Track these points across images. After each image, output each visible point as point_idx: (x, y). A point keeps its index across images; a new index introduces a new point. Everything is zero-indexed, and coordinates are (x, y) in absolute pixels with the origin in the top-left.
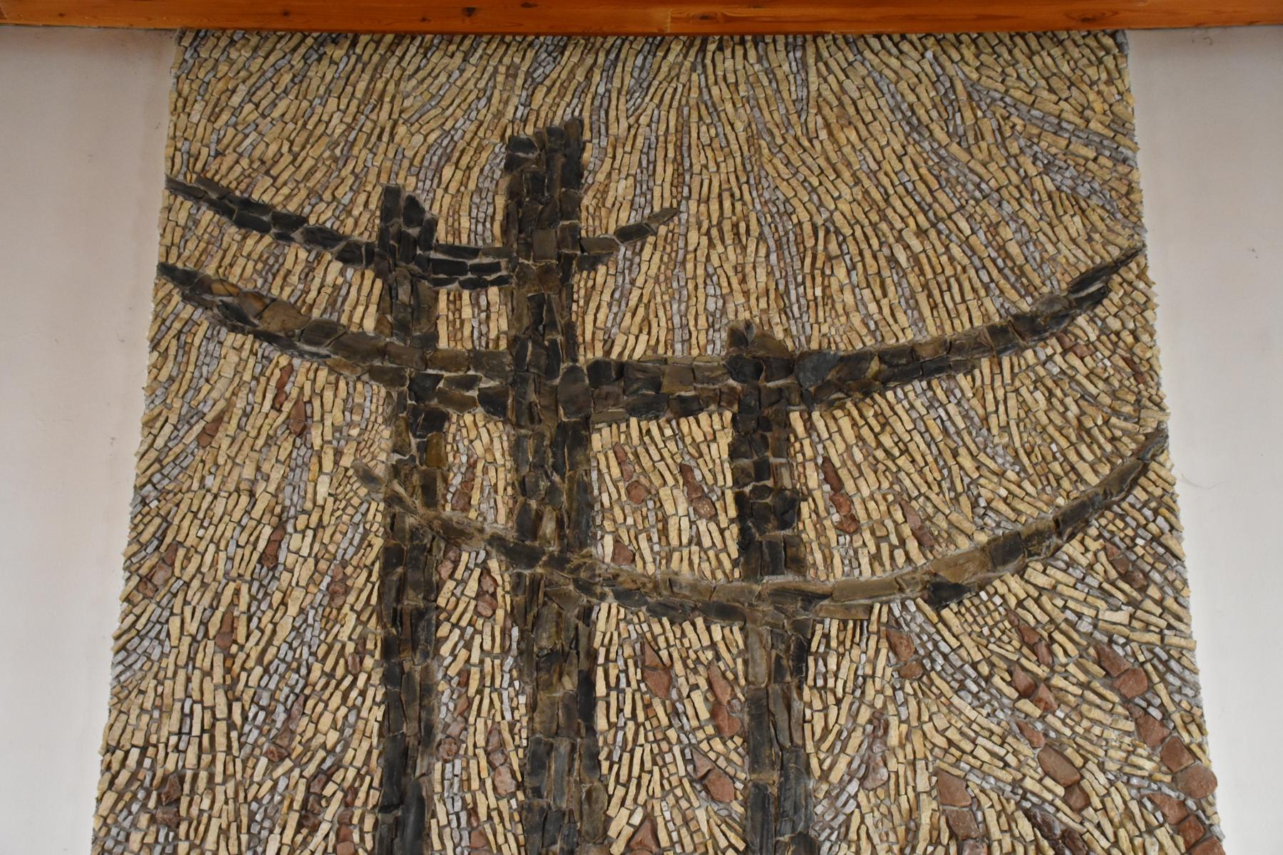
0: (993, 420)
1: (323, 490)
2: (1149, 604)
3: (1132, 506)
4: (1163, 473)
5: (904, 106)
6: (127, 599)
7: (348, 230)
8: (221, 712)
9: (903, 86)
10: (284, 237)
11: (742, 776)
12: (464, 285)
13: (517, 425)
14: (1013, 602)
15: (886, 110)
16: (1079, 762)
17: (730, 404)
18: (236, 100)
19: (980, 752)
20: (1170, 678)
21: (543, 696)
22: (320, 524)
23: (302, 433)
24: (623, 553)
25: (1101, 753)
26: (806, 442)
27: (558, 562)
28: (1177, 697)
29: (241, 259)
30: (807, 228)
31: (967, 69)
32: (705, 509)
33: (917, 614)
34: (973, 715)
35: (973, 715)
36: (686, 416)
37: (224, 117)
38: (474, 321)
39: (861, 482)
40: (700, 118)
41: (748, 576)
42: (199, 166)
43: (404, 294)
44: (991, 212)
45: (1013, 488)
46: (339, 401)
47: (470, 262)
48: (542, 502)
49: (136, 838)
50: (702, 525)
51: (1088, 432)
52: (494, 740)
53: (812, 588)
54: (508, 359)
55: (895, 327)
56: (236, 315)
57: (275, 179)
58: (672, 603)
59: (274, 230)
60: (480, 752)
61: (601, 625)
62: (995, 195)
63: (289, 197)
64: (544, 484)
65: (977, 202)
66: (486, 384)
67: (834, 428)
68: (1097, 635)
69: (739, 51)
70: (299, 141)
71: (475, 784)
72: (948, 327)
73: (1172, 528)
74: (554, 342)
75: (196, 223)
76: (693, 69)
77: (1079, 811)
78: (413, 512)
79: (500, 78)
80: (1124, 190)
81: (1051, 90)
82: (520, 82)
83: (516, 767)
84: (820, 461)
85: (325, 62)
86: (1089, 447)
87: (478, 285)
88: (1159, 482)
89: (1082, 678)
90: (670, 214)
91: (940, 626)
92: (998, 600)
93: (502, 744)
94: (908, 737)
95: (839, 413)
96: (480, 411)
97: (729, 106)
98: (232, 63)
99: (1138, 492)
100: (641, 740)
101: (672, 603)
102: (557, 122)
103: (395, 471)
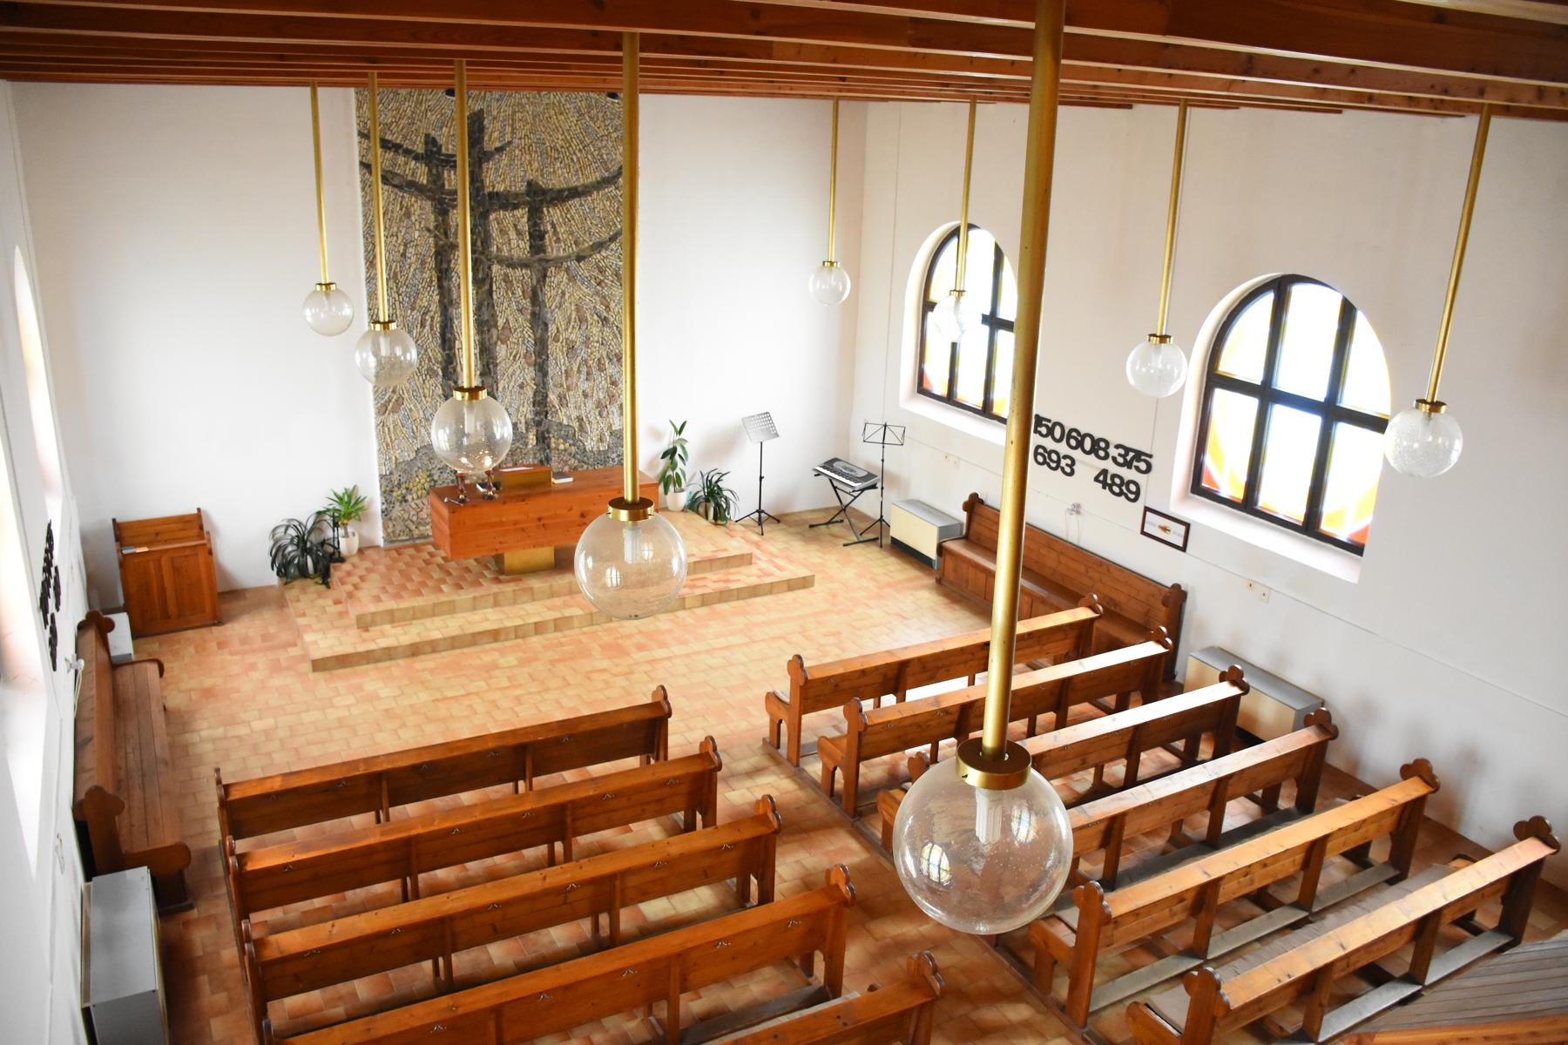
33: (574, 264)
58: (511, 264)
101: (511, 264)
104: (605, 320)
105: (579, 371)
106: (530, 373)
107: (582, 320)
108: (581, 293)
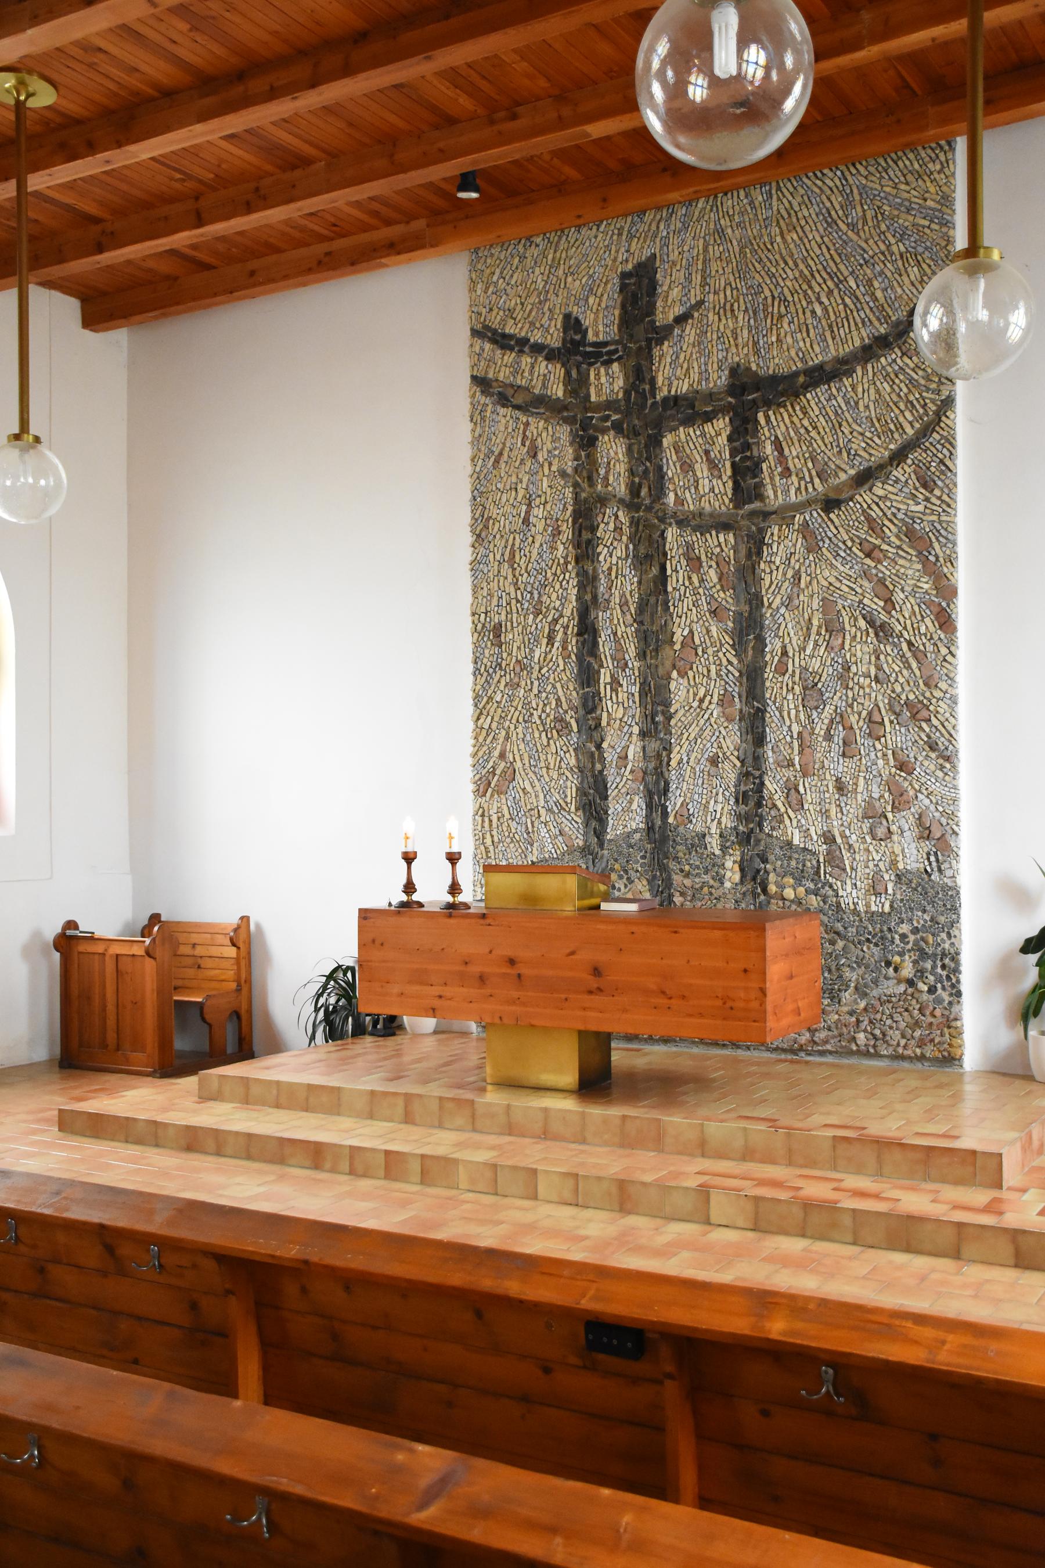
0: (861, 403)
1: (545, 485)
2: (934, 500)
3: (931, 443)
4: (948, 422)
5: (824, 211)
6: (473, 546)
7: (548, 341)
8: (513, 595)
9: (824, 197)
10: (521, 351)
11: (733, 609)
12: (603, 364)
13: (629, 439)
14: (865, 506)
15: (814, 216)
16: (891, 587)
17: (728, 412)
18: (495, 278)
19: (844, 588)
20: (941, 539)
21: (644, 577)
22: (546, 502)
23: (535, 456)
24: (680, 501)
25: (902, 582)
26: (766, 429)
27: (649, 509)
28: (944, 549)
29: (503, 367)
30: (769, 300)
31: (860, 178)
32: (716, 473)
34: (842, 569)
35: (842, 569)
36: (706, 422)
37: (491, 289)
38: (608, 382)
39: (792, 448)
40: (715, 241)
41: (737, 507)
42: (482, 319)
43: (574, 374)
44: (868, 271)
45: (869, 441)
46: (550, 438)
47: (604, 350)
48: (641, 478)
49: (487, 651)
50: (714, 481)
51: (911, 403)
52: (623, 600)
53: (767, 509)
54: (623, 403)
55: (813, 355)
56: (503, 400)
57: (515, 319)
58: (703, 523)
59: (516, 349)
60: (618, 607)
61: (669, 539)
62: (872, 261)
63: (521, 329)
64: (641, 469)
65: (861, 265)
66: (615, 417)
67: (779, 419)
68: (907, 520)
69: (735, 194)
70: (524, 295)
71: (616, 622)
72: (841, 350)
73: (951, 454)
74: (644, 390)
75: (483, 350)
76: (711, 210)
77: (889, 613)
78: (584, 491)
79: (615, 237)
80: (944, 243)
81: (907, 184)
82: (624, 237)
83: (633, 612)
84: (773, 438)
85: (533, 246)
86: (911, 412)
87: (608, 363)
88: (946, 428)
89: (898, 543)
90: (701, 303)
91: (829, 523)
92: (858, 506)
93: (627, 602)
94: (810, 583)
95: (782, 410)
96: (612, 432)
97: (729, 231)
98: (492, 255)
99: (935, 435)
100: (688, 595)
101: (703, 523)
102: (643, 258)
103: (576, 470)
104: (882, 631)
105: (828, 737)
106: (732, 739)
107: (832, 628)
108: (836, 574)
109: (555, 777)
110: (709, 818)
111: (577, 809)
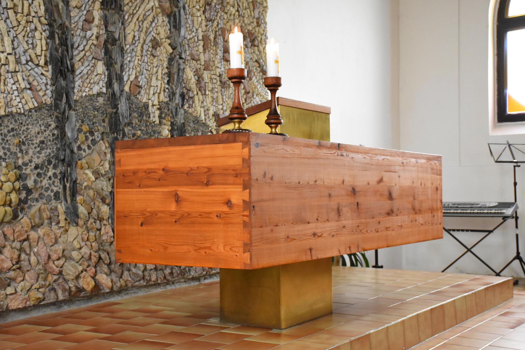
106: (162, 28)
109: (23, 22)
110: (152, 92)
111: (46, 63)
